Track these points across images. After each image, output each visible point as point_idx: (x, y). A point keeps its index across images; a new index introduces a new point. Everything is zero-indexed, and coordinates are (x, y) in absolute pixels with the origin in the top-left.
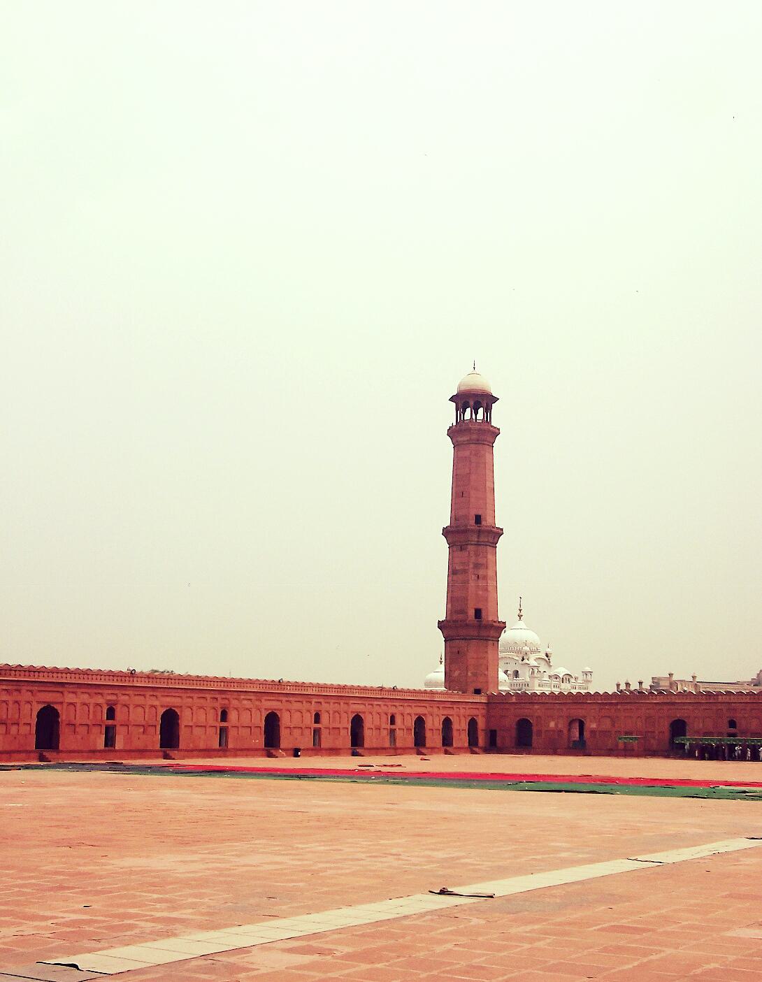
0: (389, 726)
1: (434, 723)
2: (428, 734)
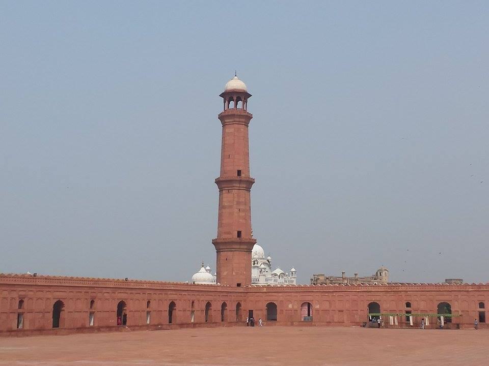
1: (216, 306)
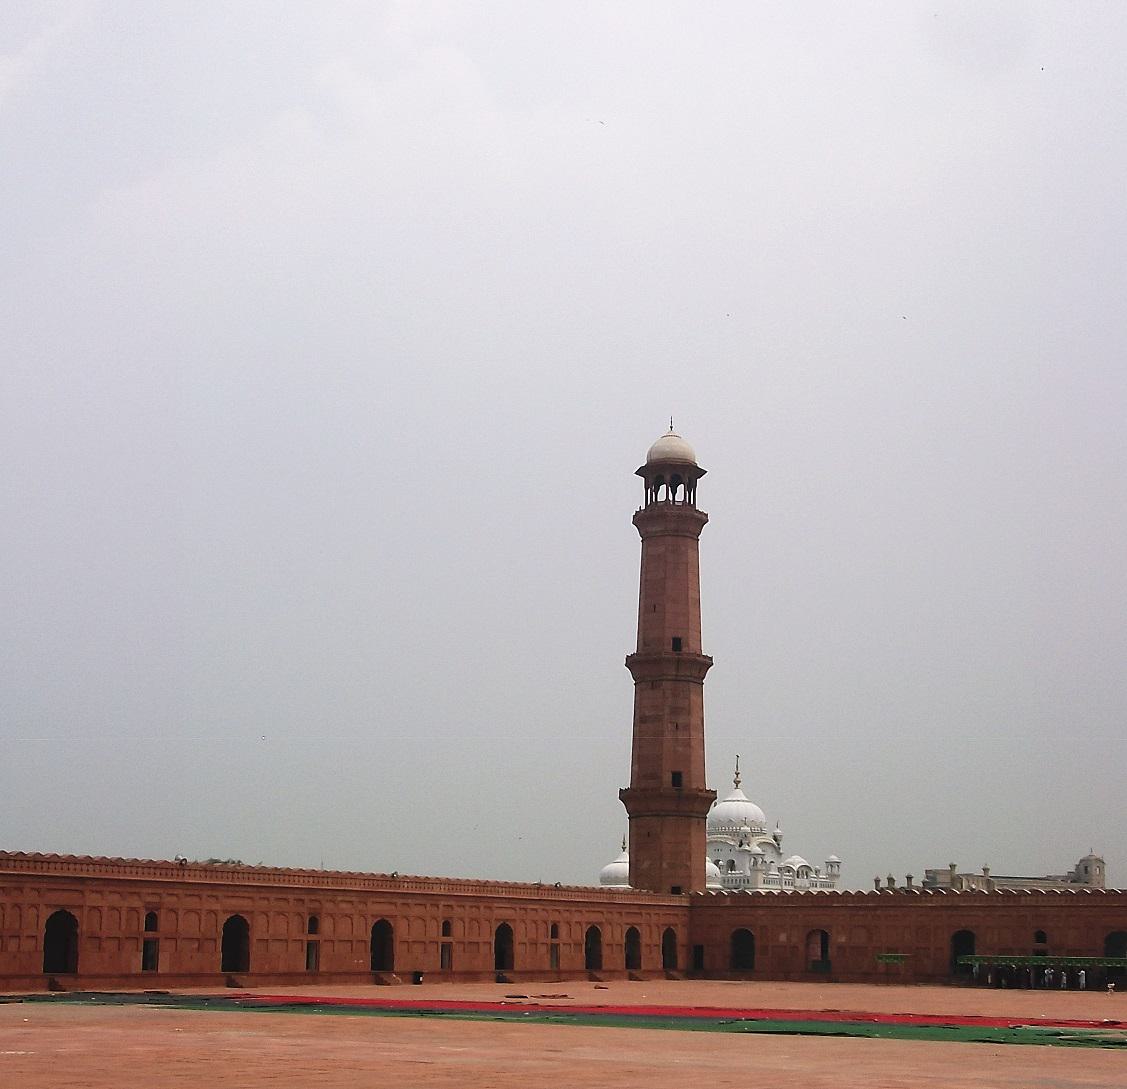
0: (549, 940)
1: (613, 936)
2: (605, 951)
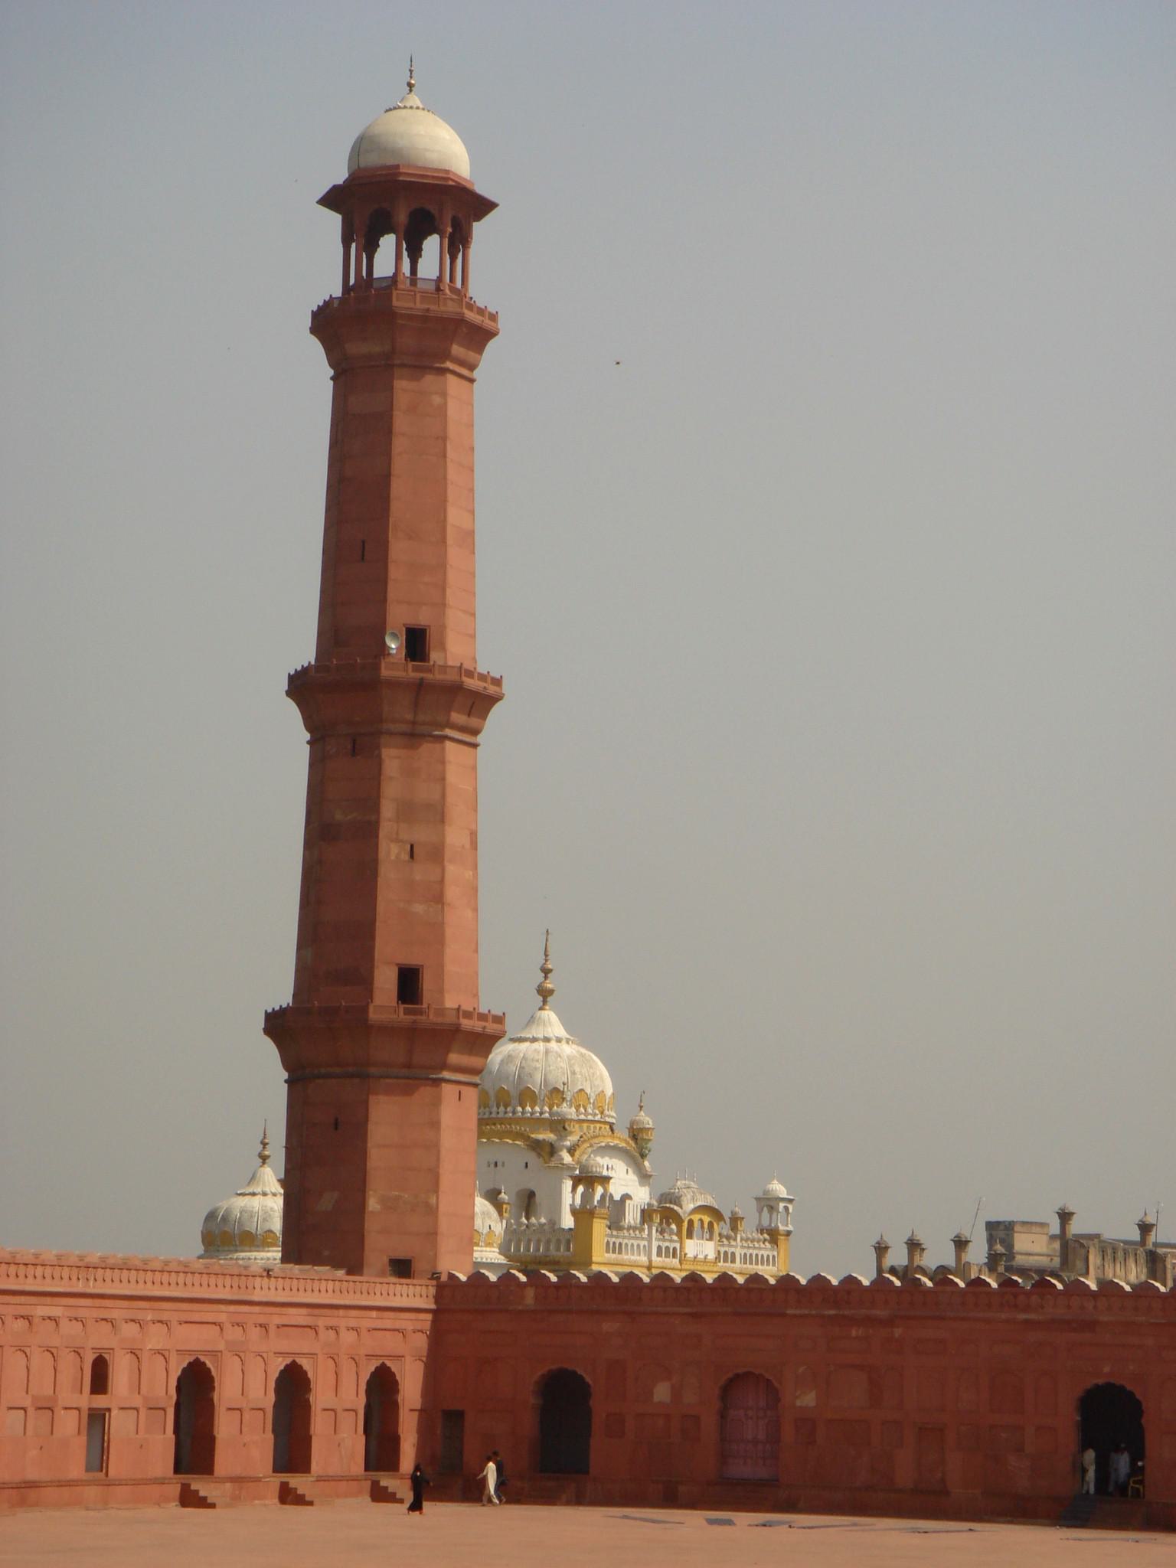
0: (86, 1400)
